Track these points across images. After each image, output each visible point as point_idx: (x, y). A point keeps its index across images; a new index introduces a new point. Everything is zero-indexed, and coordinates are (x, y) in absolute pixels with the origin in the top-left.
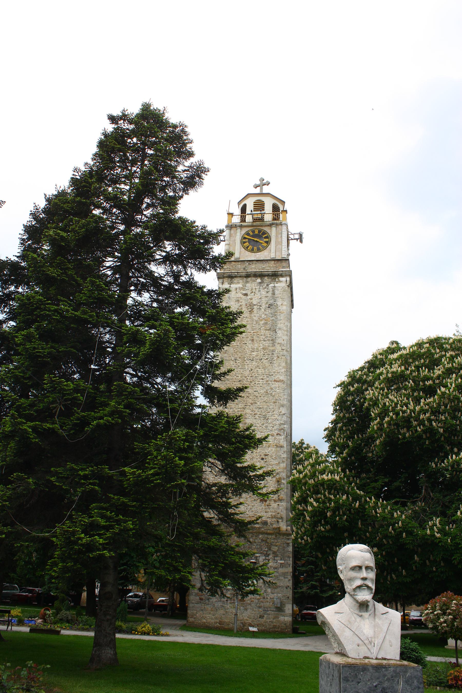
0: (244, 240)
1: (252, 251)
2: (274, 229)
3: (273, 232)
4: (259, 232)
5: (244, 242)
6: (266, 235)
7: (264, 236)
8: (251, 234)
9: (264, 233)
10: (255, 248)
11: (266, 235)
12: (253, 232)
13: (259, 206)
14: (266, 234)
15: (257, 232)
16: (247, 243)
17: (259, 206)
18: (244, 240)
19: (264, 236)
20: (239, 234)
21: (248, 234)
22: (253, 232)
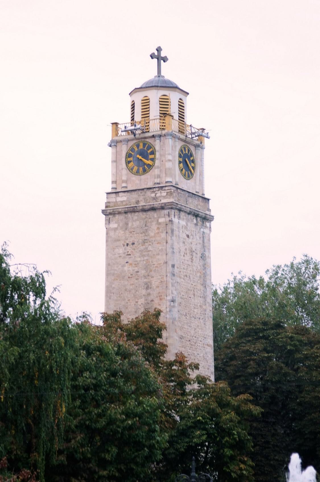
0: (129, 159)
1: (137, 173)
2: (158, 141)
3: (157, 144)
4: (144, 145)
5: (129, 162)
6: (151, 150)
7: (149, 152)
8: (136, 149)
9: (149, 147)
10: (141, 169)
11: (151, 150)
12: (138, 146)
13: (146, 103)
14: (151, 148)
15: (141, 147)
16: (132, 163)
17: (146, 103)
18: (129, 159)
19: (149, 152)
20: (124, 149)
21: (132, 149)
22: (138, 146)
